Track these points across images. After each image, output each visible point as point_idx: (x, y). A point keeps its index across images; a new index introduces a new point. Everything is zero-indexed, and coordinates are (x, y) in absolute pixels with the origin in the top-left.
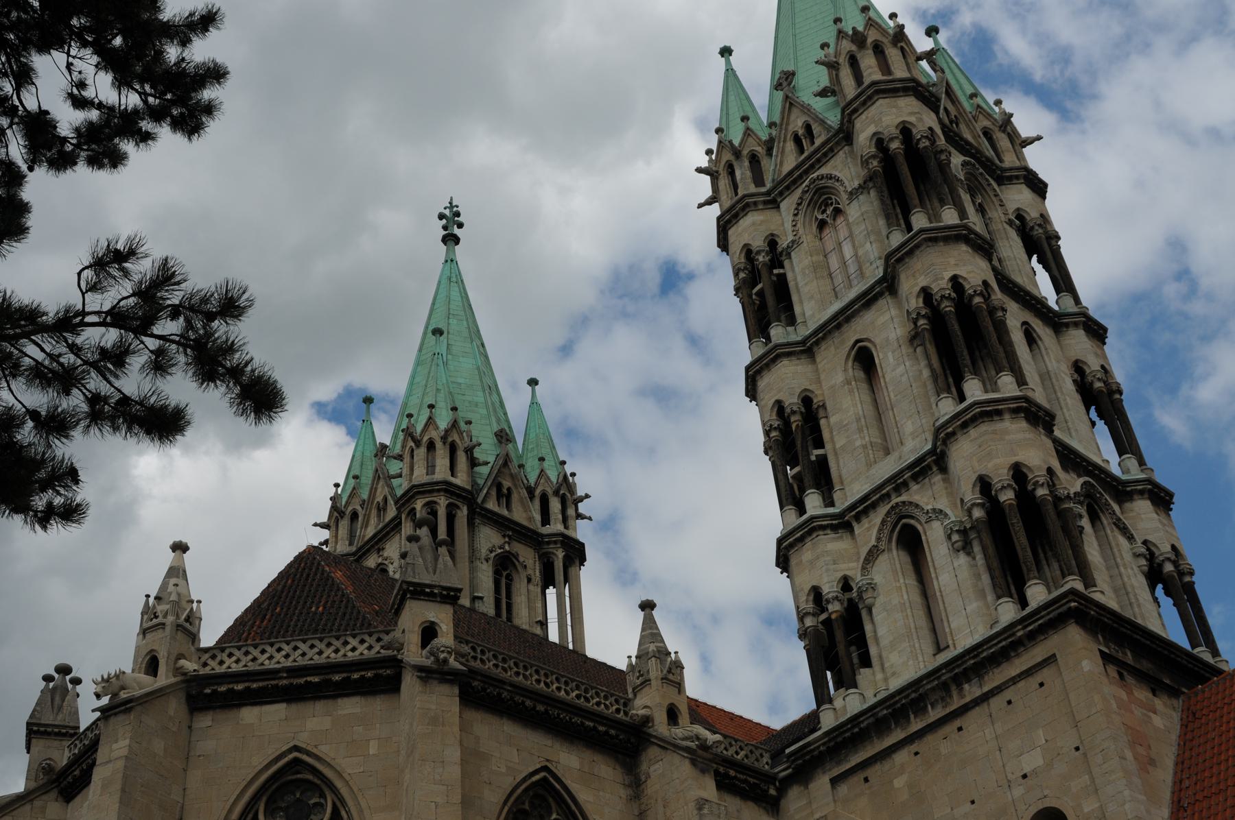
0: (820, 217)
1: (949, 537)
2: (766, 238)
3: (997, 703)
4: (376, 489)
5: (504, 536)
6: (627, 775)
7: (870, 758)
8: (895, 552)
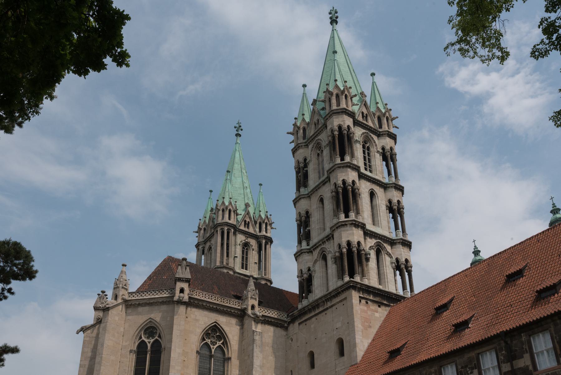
0: (318, 152)
1: (332, 259)
2: (303, 158)
3: (334, 308)
5: (246, 237)
6: (240, 322)
7: (302, 321)
8: (321, 261)
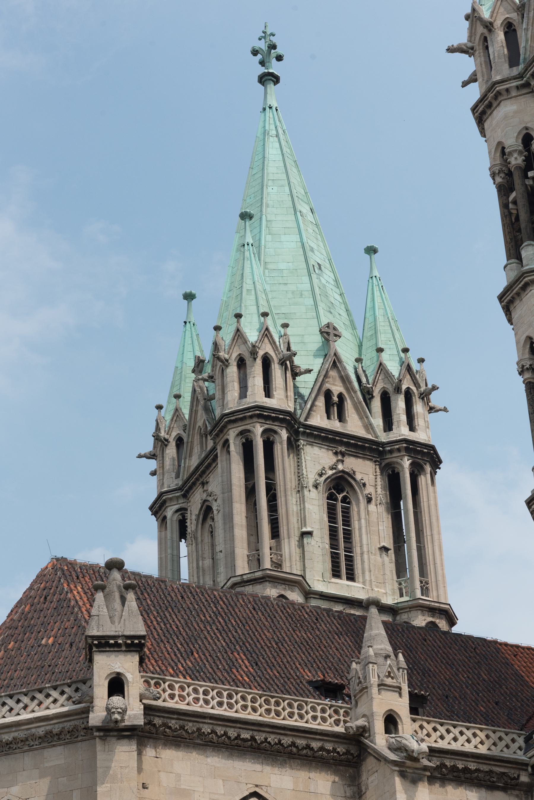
2: (519, 133)
4: (196, 412)
5: (336, 453)
6: (349, 786)
